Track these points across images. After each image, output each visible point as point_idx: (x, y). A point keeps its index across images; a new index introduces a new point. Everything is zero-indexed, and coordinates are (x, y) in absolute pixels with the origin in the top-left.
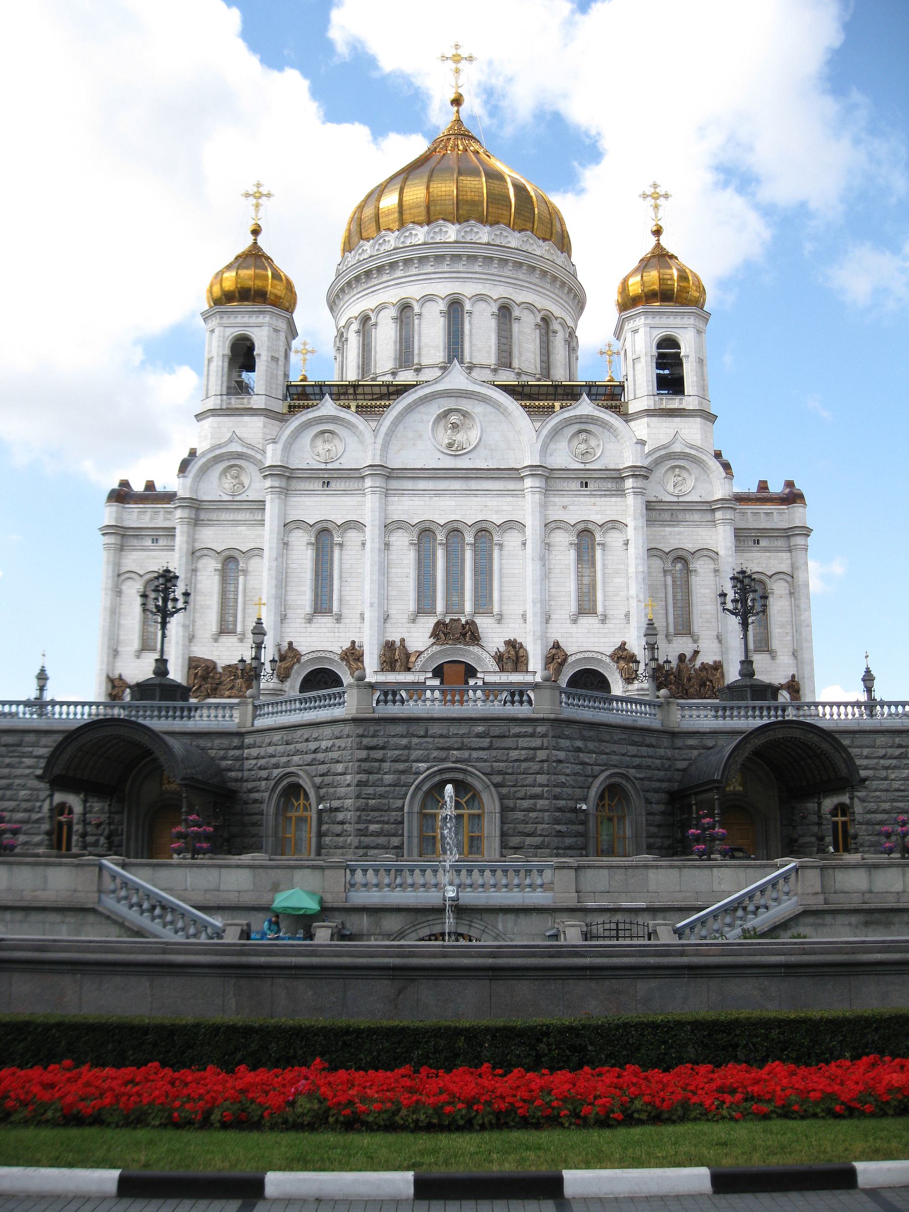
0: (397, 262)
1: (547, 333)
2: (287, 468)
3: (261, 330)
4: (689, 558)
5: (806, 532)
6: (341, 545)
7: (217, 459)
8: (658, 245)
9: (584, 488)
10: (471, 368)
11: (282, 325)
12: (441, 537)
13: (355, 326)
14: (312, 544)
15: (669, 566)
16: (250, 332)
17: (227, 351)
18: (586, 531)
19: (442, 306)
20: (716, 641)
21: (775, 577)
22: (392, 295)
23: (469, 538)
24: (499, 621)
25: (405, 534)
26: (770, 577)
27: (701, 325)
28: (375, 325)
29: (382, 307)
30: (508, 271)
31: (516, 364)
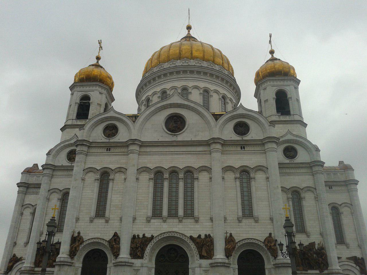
1: (225, 104)
2: (89, 142)
5: (356, 182)
6: (113, 180)
7: (66, 147)
9: (243, 149)
12: (166, 175)
13: (144, 104)
14: (98, 180)
16: (88, 93)
17: (78, 101)
19: (179, 91)
20: (320, 236)
21: (343, 205)
22: (158, 89)
24: (197, 221)
25: (148, 174)
26: (341, 205)
29: (154, 94)
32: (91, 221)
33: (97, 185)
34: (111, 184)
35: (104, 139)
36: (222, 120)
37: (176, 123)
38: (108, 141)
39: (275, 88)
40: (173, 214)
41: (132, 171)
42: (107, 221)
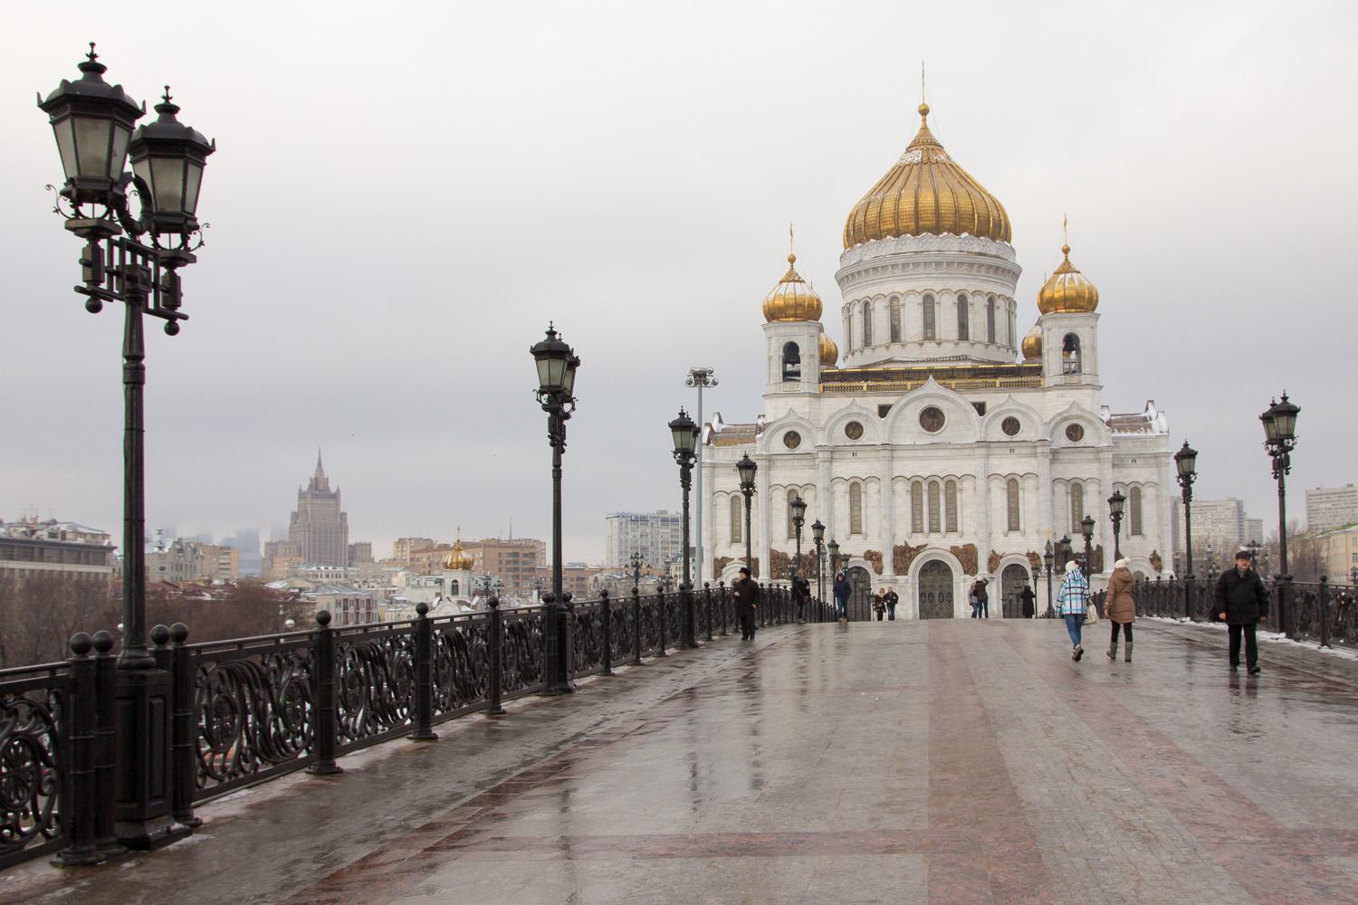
0: (887, 266)
3: (800, 334)
4: (1083, 484)
6: (866, 492)
8: (1067, 260)
10: (939, 344)
11: (814, 331)
12: (925, 487)
13: (857, 308)
15: (1070, 491)
16: (795, 340)
18: (1014, 480)
19: (921, 301)
23: (942, 486)
27: (1092, 323)
28: (873, 309)
30: (963, 270)
31: (971, 337)
32: (849, 539)
33: (848, 497)
34: (863, 496)
35: (850, 442)
36: (987, 416)
37: (932, 419)
38: (853, 444)
39: (1063, 330)
40: (934, 529)
41: (885, 483)
42: (866, 539)
